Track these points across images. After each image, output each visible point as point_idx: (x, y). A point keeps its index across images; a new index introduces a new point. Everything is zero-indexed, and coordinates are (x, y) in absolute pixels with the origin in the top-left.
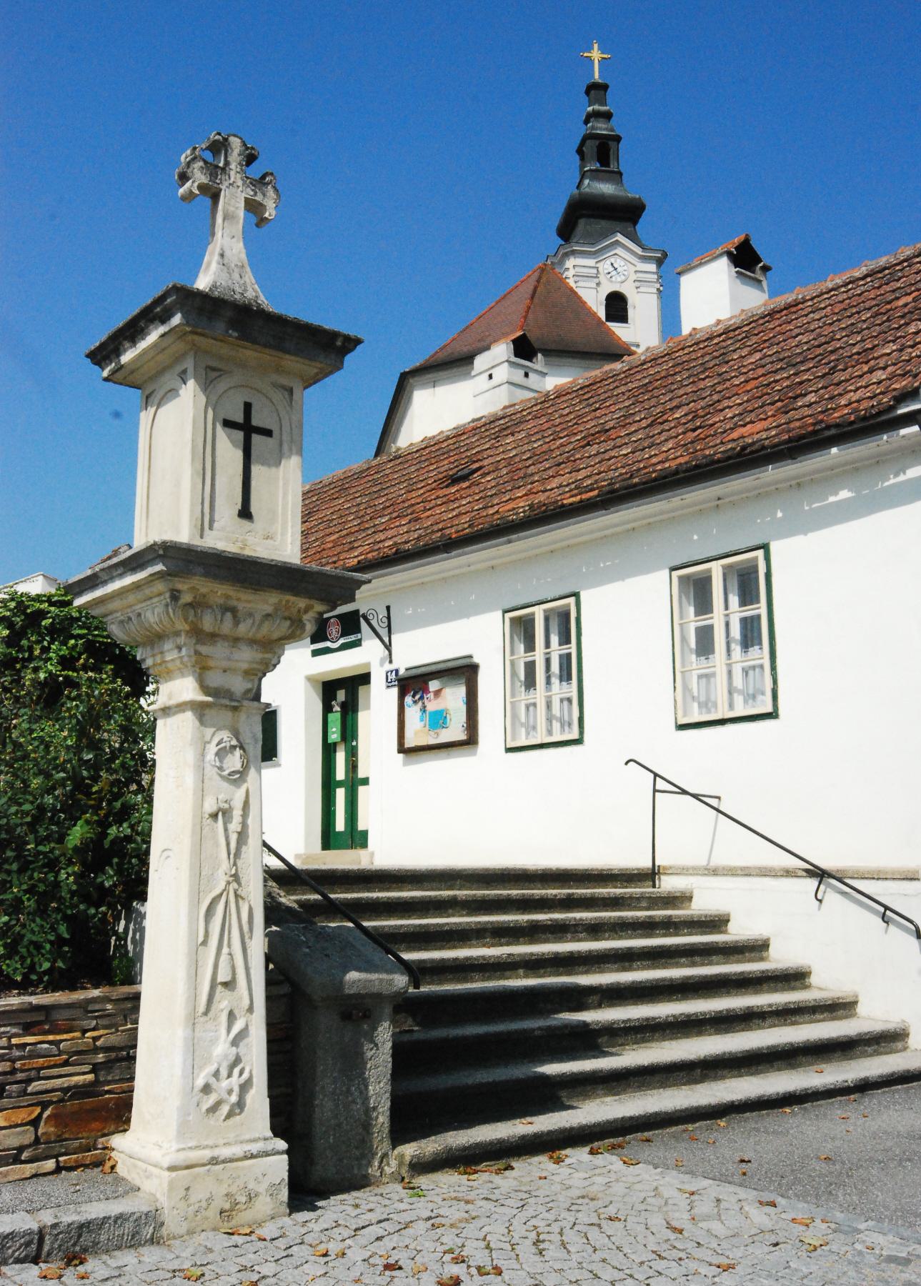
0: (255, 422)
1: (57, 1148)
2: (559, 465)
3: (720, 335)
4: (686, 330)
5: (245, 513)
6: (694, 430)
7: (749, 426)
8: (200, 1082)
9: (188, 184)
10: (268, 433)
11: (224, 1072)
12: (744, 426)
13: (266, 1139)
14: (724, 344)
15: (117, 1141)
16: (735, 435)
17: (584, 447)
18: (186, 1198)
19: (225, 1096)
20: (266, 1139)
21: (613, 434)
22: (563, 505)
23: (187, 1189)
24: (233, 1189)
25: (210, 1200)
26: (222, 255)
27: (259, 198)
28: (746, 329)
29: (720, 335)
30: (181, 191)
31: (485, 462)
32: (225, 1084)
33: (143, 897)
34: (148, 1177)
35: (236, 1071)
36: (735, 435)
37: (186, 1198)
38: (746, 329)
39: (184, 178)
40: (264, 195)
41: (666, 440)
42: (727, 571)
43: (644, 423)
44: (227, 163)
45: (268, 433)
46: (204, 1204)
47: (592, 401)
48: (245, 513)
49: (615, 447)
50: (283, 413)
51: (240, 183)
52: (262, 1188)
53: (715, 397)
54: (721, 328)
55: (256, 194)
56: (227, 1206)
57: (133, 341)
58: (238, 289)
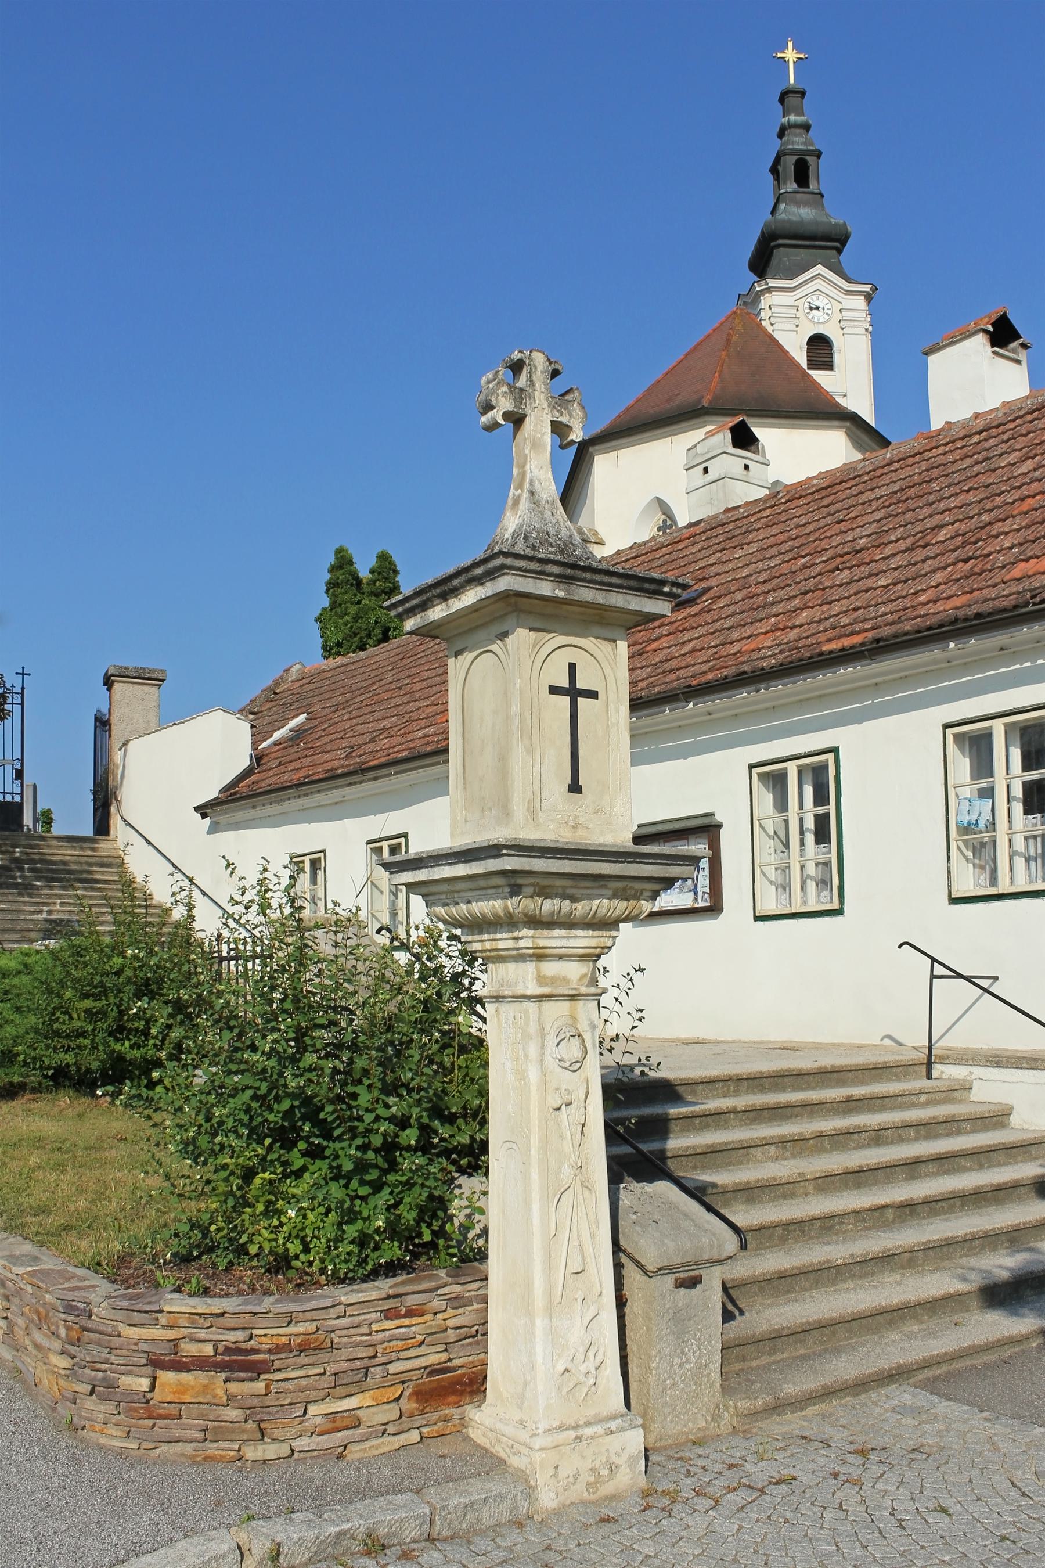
0: (580, 685)
1: (419, 1421)
2: (806, 593)
3: (980, 433)
4: (936, 423)
5: (575, 787)
6: (965, 561)
7: (1033, 561)
8: (561, 1368)
9: (492, 414)
10: (593, 695)
11: (580, 1357)
12: (1027, 560)
13: (622, 1416)
14: (986, 445)
15: (472, 1413)
16: (1017, 572)
17: (833, 571)
18: (555, 1475)
19: (582, 1379)
20: (622, 1416)
21: (866, 556)
22: (821, 654)
23: (556, 1467)
24: (597, 1464)
25: (576, 1476)
26: (532, 493)
27: (564, 419)
28: (1012, 426)
29: (980, 433)
30: (484, 419)
31: (713, 582)
32: (583, 1368)
33: (474, 1158)
34: (514, 1454)
35: (591, 1353)
36: (1017, 572)
37: (555, 1475)
38: (1012, 426)
39: (488, 407)
40: (570, 415)
41: (934, 571)
42: (1009, 728)
43: (902, 545)
44: (532, 383)
45: (593, 695)
46: (571, 1479)
47: (833, 509)
48: (575, 787)
49: (870, 575)
50: (608, 670)
51: (546, 405)
52: (620, 1461)
53: (985, 518)
54: (980, 424)
55: (562, 414)
56: (592, 1479)
57: (444, 597)
58: (552, 532)
